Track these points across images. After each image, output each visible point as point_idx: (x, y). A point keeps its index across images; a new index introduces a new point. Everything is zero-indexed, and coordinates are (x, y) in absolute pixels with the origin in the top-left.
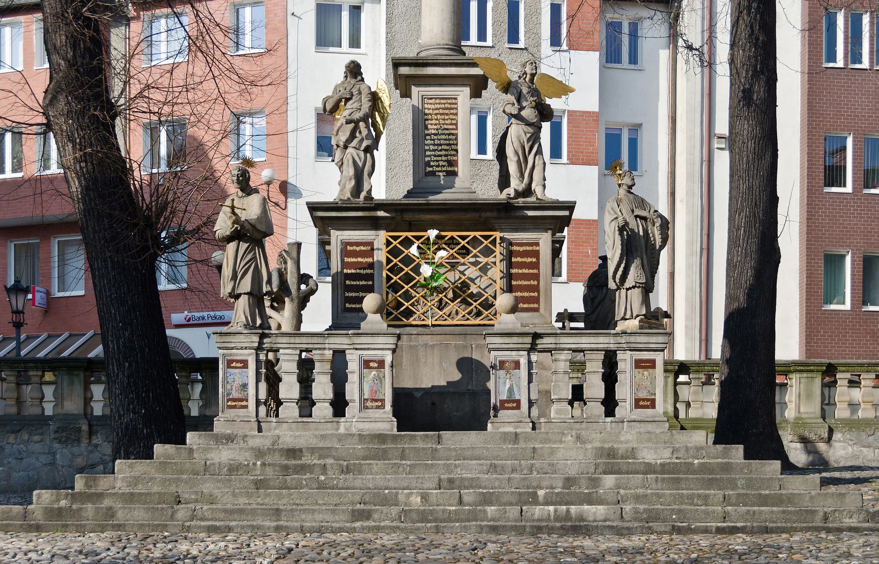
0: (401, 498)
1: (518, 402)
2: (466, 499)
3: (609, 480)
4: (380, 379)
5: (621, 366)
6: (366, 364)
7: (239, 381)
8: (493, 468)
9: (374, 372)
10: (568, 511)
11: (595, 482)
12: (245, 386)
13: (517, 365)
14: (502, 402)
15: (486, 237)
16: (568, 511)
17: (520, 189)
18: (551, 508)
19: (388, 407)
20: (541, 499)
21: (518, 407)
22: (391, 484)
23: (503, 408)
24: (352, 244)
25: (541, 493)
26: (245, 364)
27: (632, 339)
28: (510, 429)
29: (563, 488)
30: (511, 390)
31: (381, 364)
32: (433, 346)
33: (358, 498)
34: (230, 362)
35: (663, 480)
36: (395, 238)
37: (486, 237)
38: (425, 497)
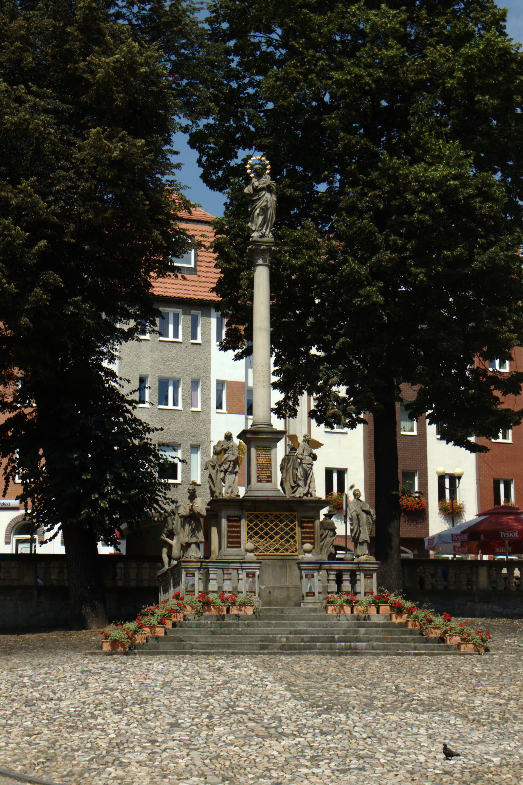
0: (278, 639)
1: (314, 593)
2: (305, 639)
3: (362, 630)
4: (253, 582)
5: (358, 577)
6: (247, 575)
7: (191, 582)
8: (311, 625)
9: (251, 579)
10: (350, 645)
11: (356, 632)
12: (193, 585)
13: (313, 576)
14: (307, 593)
15: (292, 515)
16: (350, 645)
17: (305, 492)
18: (343, 644)
19: (257, 595)
20: (336, 639)
21: (314, 595)
22: (270, 632)
23: (307, 595)
24: (231, 517)
25: (336, 636)
26: (194, 575)
27: (363, 565)
28: (311, 606)
29: (344, 634)
30: (310, 588)
31: (254, 575)
32: (269, 565)
33: (259, 639)
34: (187, 574)
35: (385, 631)
36: (251, 515)
37: (292, 515)
38: (287, 638)
